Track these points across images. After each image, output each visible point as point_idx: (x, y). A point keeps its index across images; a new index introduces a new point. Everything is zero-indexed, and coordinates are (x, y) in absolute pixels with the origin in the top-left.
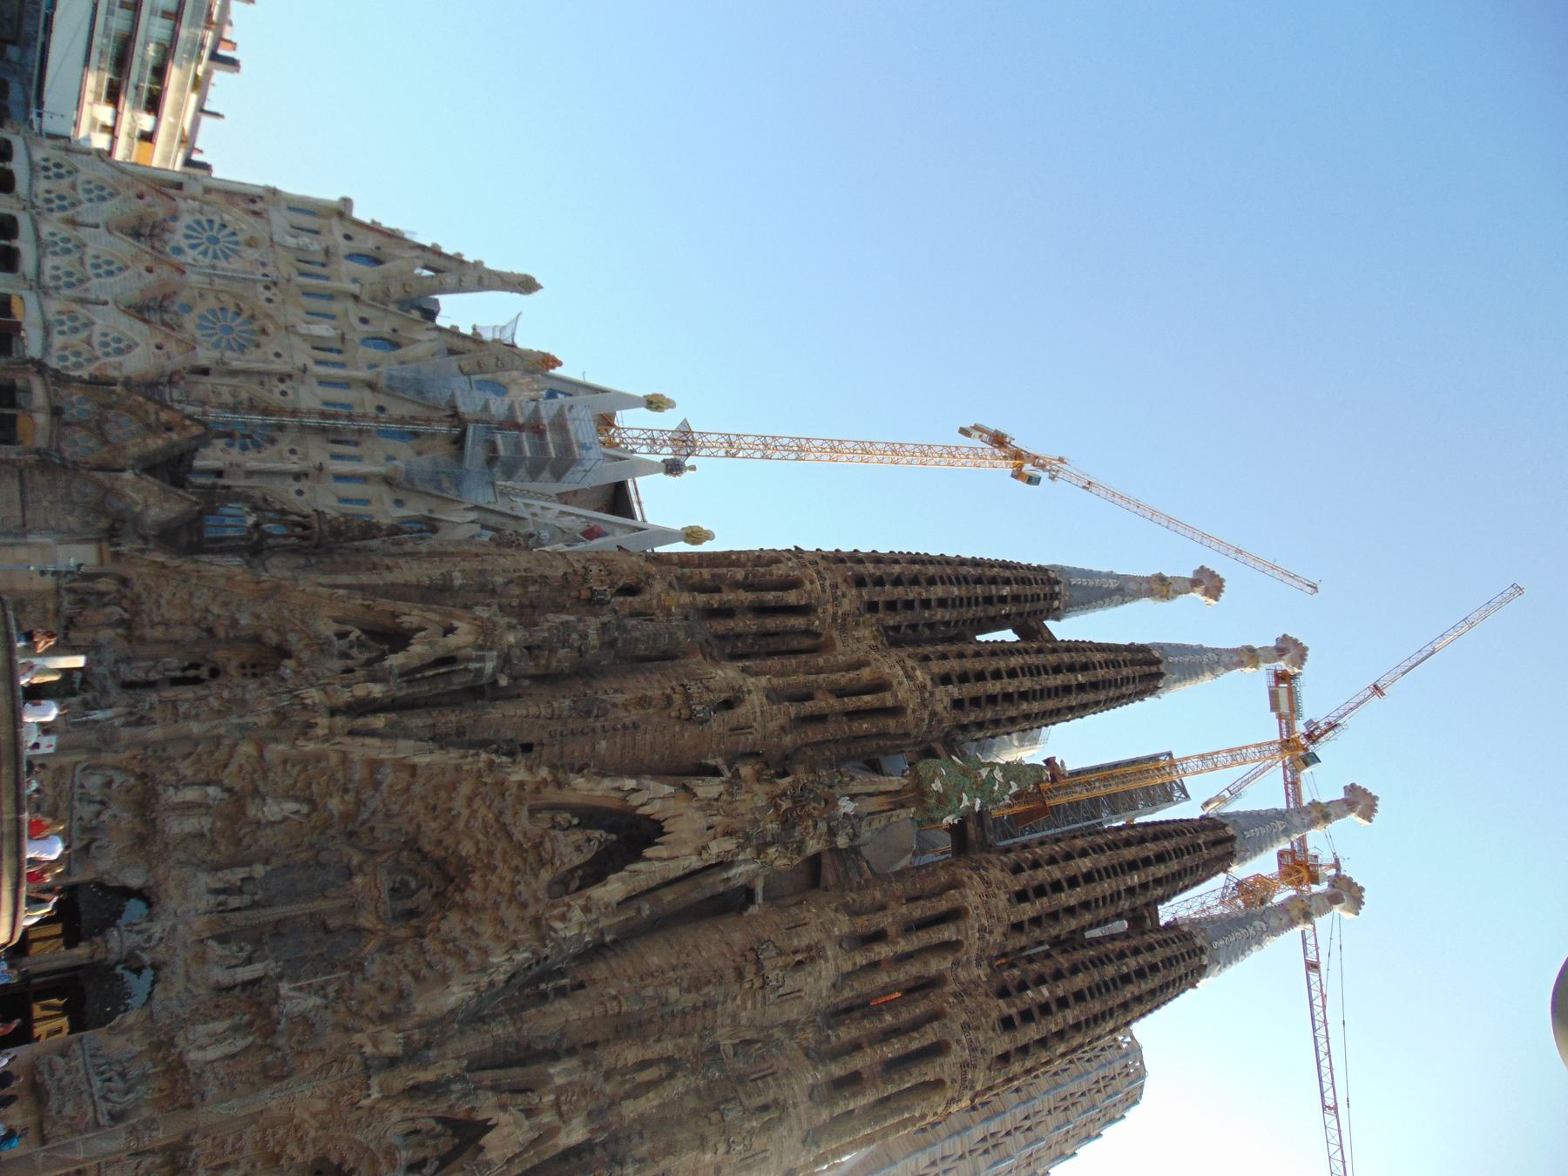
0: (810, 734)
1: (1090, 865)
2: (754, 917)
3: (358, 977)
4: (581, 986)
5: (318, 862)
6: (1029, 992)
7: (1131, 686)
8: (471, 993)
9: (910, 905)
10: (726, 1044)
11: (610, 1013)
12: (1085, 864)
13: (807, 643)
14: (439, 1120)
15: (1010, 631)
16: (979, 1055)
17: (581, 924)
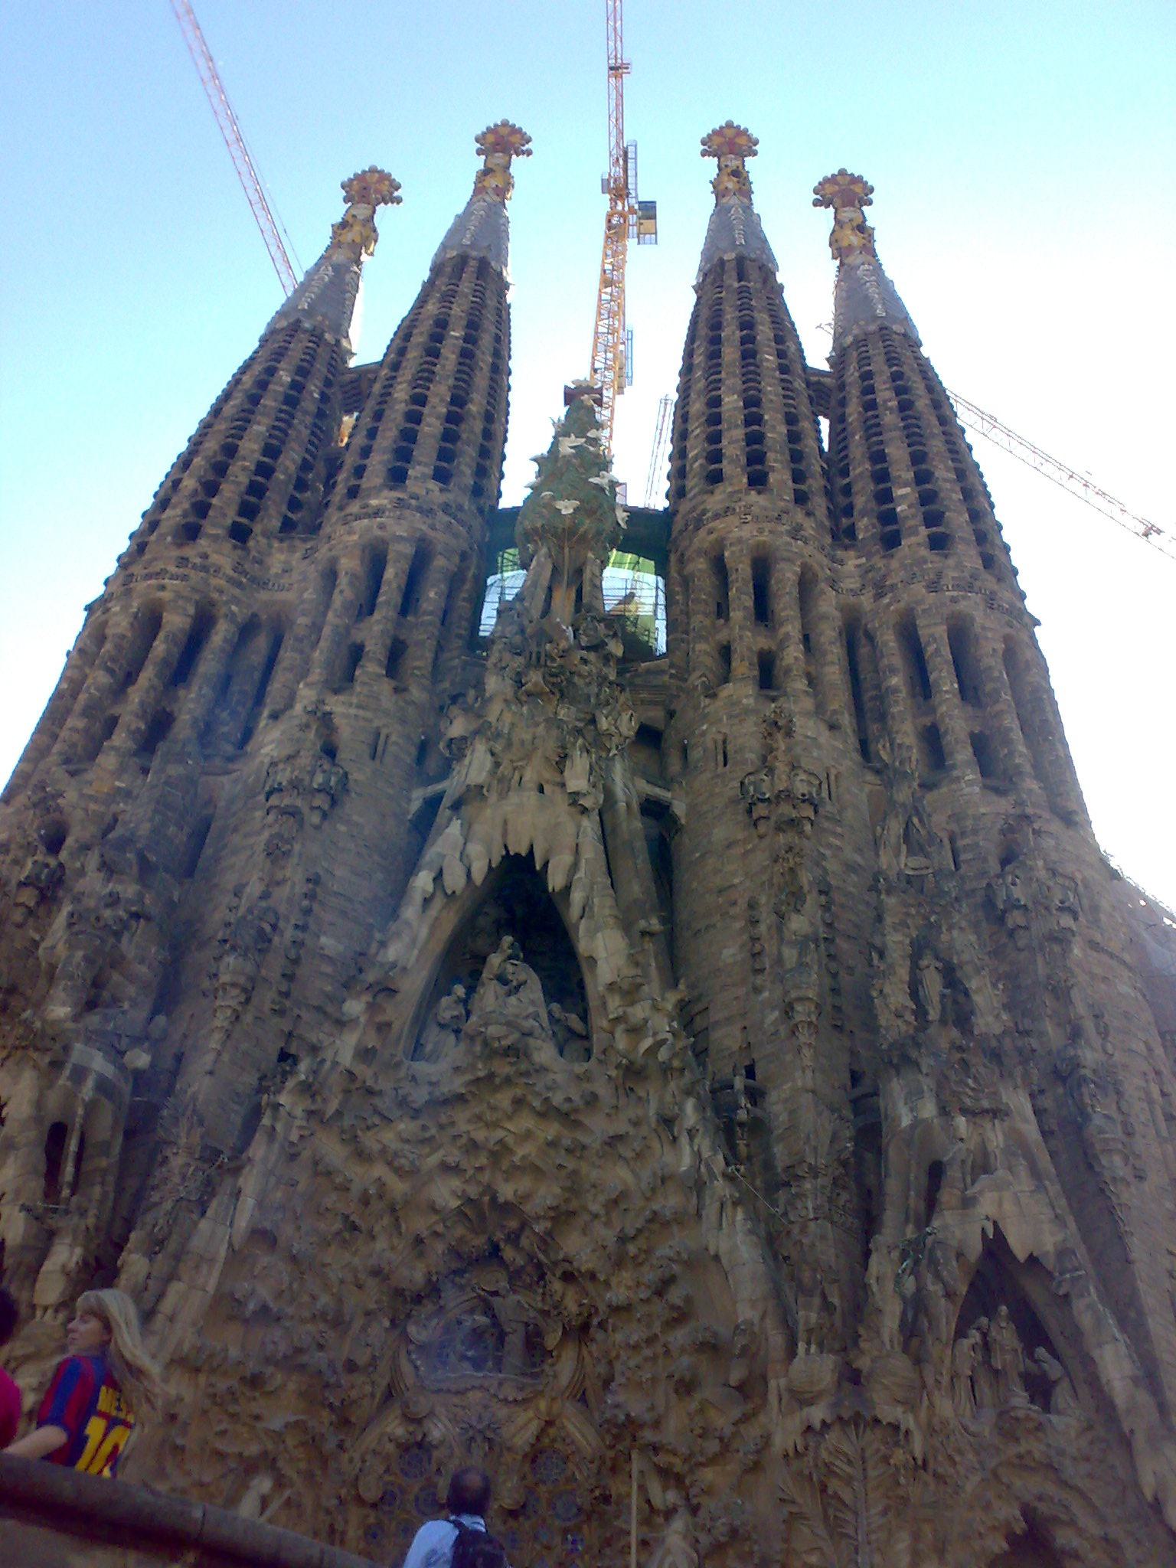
0: (417, 663)
1: (736, 397)
2: (692, 808)
3: (648, 1435)
5: (374, 1506)
6: (899, 509)
7: (488, 294)
8: (740, 1215)
10: (908, 863)
11: (814, 1018)
12: (731, 402)
13: (261, 643)
14: (960, 1333)
15: (346, 419)
16: (978, 584)
17: (655, 1008)
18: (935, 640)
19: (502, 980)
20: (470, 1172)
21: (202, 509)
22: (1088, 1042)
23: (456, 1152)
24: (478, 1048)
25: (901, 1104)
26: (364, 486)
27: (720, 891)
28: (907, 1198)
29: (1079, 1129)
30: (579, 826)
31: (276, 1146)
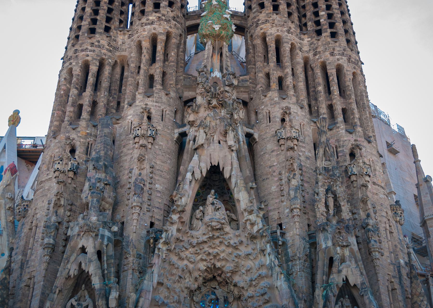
0: (172, 82)
2: (260, 136)
4: (280, 225)
6: (321, 21)
8: (282, 276)
9: (270, 61)
14: (336, 303)
16: (345, 53)
17: (257, 216)
18: (332, 75)
19: (213, 204)
20: (209, 260)
21: (94, 21)
22: (371, 218)
23: (205, 256)
24: (210, 228)
25: (322, 241)
26: (146, 10)
27: (270, 167)
28: (324, 268)
29: (368, 243)
30: (232, 156)
31: (160, 259)
